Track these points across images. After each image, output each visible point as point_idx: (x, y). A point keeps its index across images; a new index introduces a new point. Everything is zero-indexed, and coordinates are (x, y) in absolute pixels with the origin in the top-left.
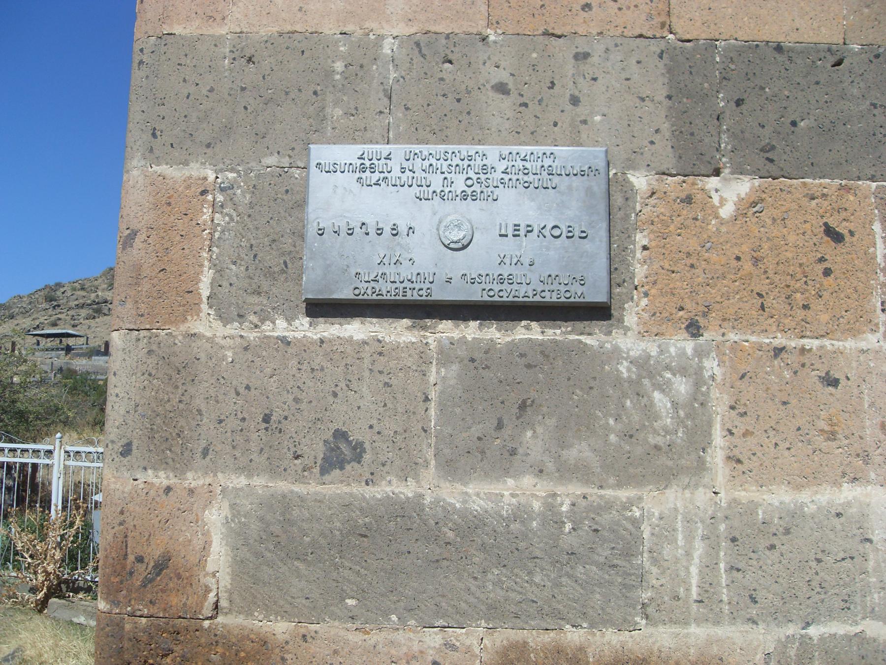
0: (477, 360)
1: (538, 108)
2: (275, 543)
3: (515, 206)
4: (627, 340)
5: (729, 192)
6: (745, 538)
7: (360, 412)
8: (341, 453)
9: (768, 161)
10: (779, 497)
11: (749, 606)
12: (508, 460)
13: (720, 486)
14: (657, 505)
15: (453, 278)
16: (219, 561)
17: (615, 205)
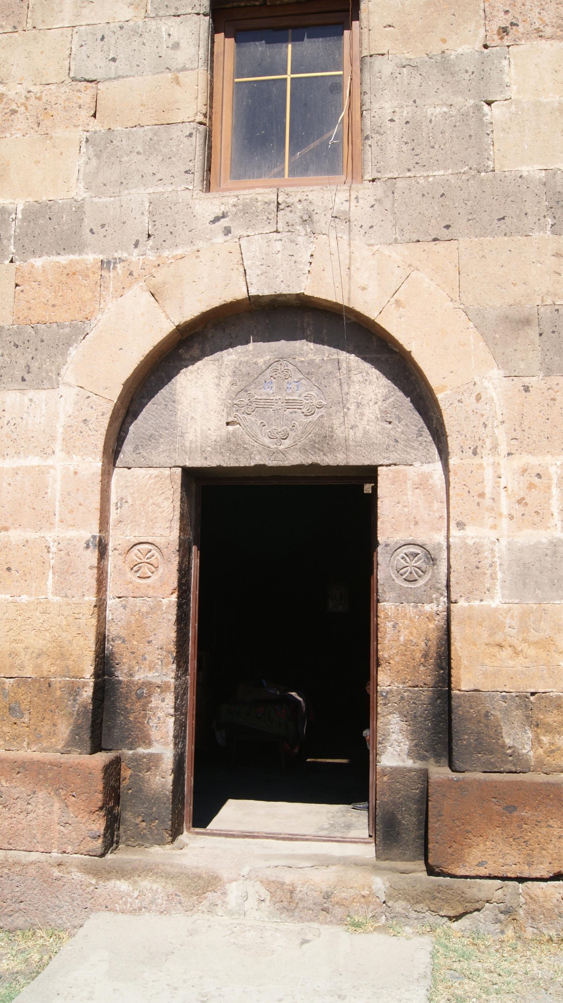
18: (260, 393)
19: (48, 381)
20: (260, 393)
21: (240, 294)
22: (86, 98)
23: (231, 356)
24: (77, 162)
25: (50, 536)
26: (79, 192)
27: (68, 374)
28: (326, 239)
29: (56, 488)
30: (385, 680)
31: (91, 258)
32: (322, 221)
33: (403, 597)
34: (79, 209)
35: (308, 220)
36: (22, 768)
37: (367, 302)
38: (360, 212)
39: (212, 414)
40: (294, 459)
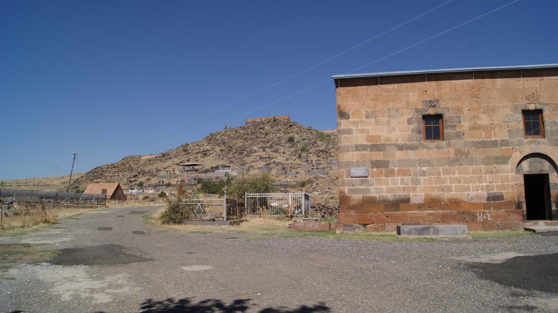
0: (361, 180)
1: (363, 165)
2: (350, 190)
3: (362, 171)
4: (369, 178)
5: (375, 169)
6: (376, 189)
7: (354, 183)
8: (353, 185)
9: (377, 167)
10: (378, 187)
11: (376, 193)
12: (362, 185)
13: (375, 186)
14: (371, 187)
15: (359, 175)
16: (347, 192)
17: (368, 171)
18: (533, 165)
19: (507, 164)
20: (533, 165)
21: (531, 152)
22: (506, 124)
23: (529, 160)
24: (507, 134)
25: (510, 183)
26: (508, 138)
27: (509, 162)
28: (542, 146)
29: (510, 177)
30: (552, 199)
31: (511, 147)
32: (541, 143)
33: (553, 189)
34: (508, 141)
35: (539, 143)
36: (512, 212)
37: (548, 154)
38: (546, 142)
39: (526, 166)
40: (538, 173)
